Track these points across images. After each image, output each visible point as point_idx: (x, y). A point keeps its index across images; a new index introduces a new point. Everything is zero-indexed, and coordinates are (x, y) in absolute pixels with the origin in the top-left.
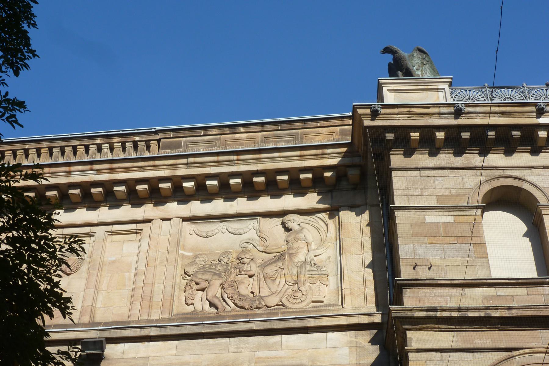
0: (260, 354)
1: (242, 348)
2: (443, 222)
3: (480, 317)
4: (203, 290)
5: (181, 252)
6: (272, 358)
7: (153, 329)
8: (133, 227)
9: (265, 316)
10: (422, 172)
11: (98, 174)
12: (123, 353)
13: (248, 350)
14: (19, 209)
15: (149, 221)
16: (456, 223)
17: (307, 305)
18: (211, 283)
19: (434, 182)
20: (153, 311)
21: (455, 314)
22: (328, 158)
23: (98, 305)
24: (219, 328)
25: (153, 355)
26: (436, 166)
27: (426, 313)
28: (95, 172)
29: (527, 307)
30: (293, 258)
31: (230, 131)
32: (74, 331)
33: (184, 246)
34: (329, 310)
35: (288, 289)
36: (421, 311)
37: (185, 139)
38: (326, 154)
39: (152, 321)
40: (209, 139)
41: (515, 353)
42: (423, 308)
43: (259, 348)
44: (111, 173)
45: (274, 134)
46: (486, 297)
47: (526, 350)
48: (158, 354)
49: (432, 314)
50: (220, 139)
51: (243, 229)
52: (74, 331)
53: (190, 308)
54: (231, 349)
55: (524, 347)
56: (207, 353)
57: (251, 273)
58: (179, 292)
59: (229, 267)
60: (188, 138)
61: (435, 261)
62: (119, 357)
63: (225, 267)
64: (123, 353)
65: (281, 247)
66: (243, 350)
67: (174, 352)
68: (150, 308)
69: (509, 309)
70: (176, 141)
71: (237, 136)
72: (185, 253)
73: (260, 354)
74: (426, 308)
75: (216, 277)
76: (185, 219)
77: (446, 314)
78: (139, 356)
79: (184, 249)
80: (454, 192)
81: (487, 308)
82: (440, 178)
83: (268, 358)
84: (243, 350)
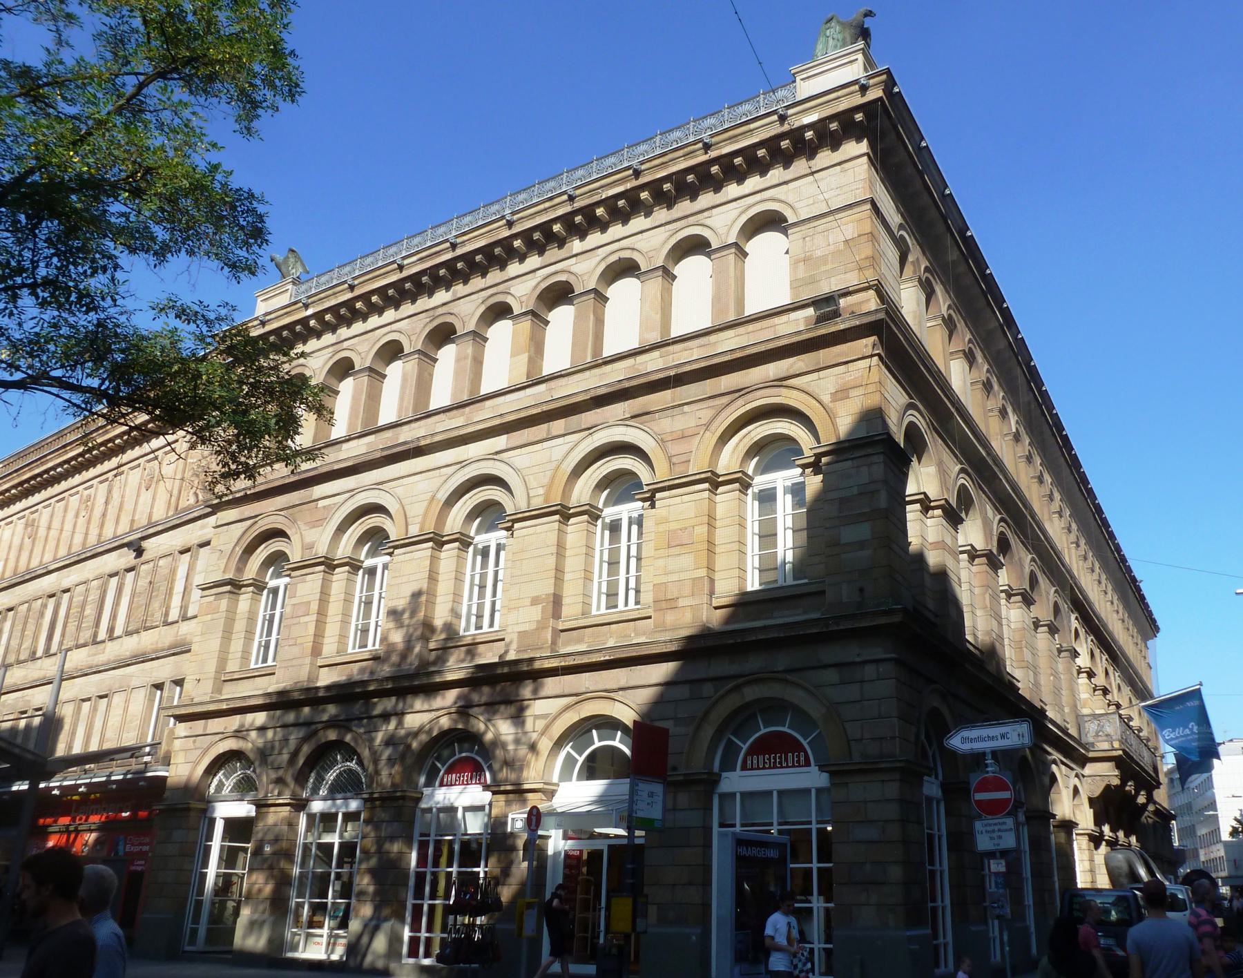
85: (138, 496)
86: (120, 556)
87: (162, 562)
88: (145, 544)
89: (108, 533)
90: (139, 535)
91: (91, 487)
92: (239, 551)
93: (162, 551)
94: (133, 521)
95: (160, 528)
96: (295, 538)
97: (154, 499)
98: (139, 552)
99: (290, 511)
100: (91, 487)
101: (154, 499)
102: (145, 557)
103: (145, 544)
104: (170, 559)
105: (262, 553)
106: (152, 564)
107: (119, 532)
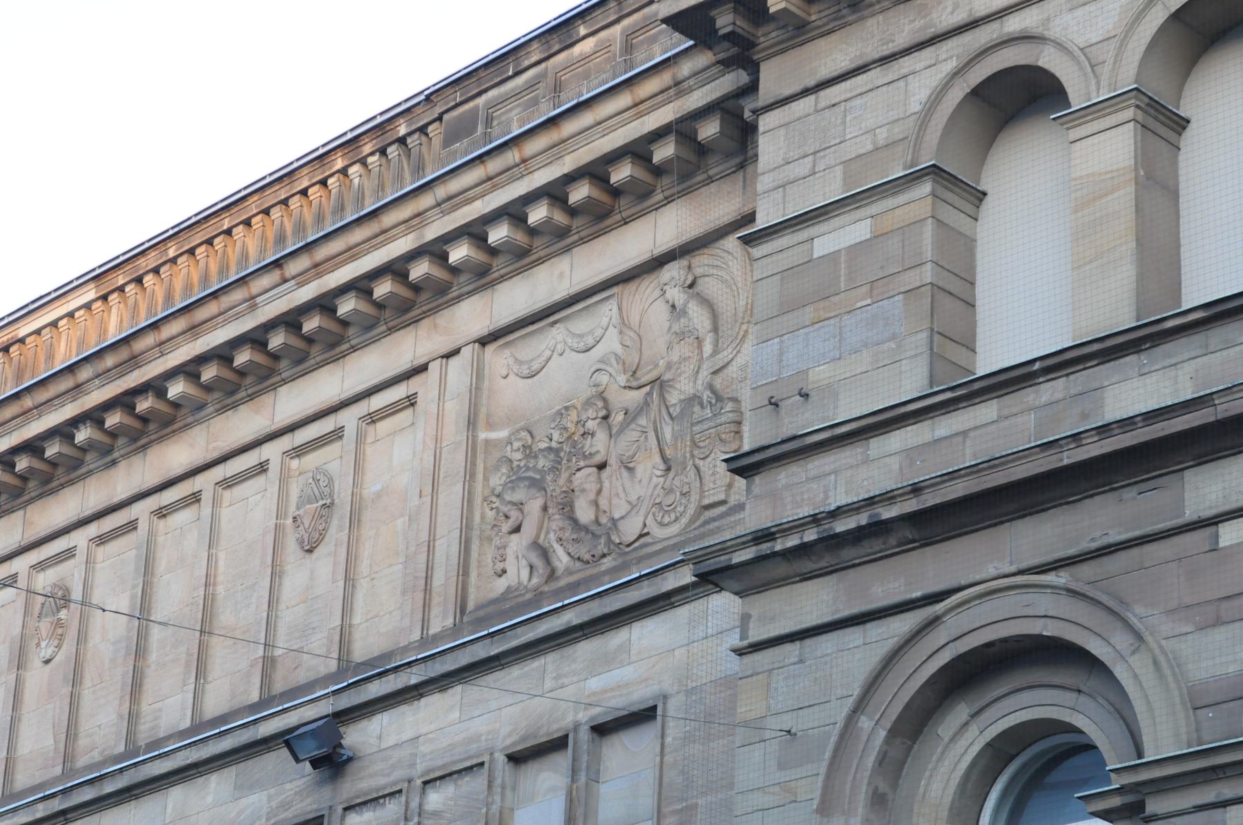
0: (594, 684)
1: (566, 676)
2: (848, 244)
3: (860, 529)
4: (517, 530)
5: (483, 435)
6: (612, 690)
7: (414, 669)
8: (397, 393)
9: (607, 578)
10: (822, 94)
11: (301, 285)
12: (380, 738)
13: (575, 679)
14: (657, 158)
15: (422, 369)
16: (877, 237)
17: (692, 521)
18: (526, 508)
19: (844, 123)
20: (435, 611)
21: (811, 535)
22: (691, 90)
23: (357, 620)
24: (516, 637)
25: (424, 731)
26: (853, 66)
27: (754, 549)
28: (293, 282)
29: (952, 475)
30: (667, 395)
31: (560, 42)
32: (295, 707)
33: (488, 416)
34: (719, 530)
35: (656, 486)
36: (744, 545)
37: (484, 98)
38: (684, 81)
39: (437, 639)
40: (526, 82)
41: (939, 607)
42: (744, 539)
43: (593, 670)
44: (319, 275)
45: (645, 18)
46: (909, 453)
47: (977, 588)
48: (433, 727)
49: (765, 548)
50: (544, 75)
51: (591, 332)
52: (295, 707)
53: (501, 585)
54: (549, 684)
55: (963, 583)
56: (510, 701)
57: (598, 459)
58: (481, 545)
59: (562, 454)
60: (491, 94)
61: (820, 374)
62: (375, 749)
63: (552, 457)
64: (380, 738)
65: (657, 366)
66: (566, 681)
67: (457, 714)
68: (426, 606)
69: (916, 489)
70: (465, 112)
71: (577, 50)
72: (494, 435)
73: (594, 684)
74: (750, 538)
75: (533, 491)
76: (484, 342)
77: (792, 541)
78: (405, 737)
79: (491, 426)
80: (882, 136)
81: (871, 501)
82: (858, 101)
83: (606, 691)
84: (566, 681)
85: (276, 574)
86: (242, 788)
87: (435, 799)
88: (356, 736)
89: (169, 708)
90: (325, 708)
91: (69, 554)
92: (874, 731)
93: (430, 757)
94: (269, 664)
95: (413, 677)
96: (1131, 671)
97: (350, 581)
98: (331, 762)
99: (1087, 570)
100: (69, 554)
101: (350, 581)
102: (357, 784)
103: (356, 736)
104: (474, 784)
105: (962, 738)
106: (392, 808)
107: (214, 705)
